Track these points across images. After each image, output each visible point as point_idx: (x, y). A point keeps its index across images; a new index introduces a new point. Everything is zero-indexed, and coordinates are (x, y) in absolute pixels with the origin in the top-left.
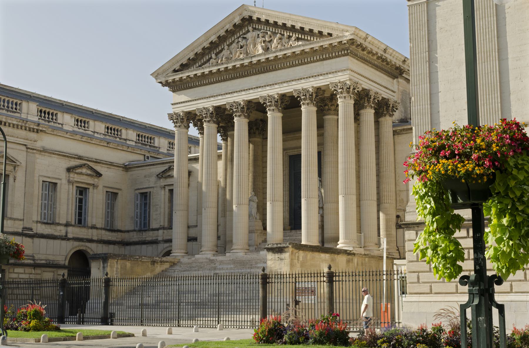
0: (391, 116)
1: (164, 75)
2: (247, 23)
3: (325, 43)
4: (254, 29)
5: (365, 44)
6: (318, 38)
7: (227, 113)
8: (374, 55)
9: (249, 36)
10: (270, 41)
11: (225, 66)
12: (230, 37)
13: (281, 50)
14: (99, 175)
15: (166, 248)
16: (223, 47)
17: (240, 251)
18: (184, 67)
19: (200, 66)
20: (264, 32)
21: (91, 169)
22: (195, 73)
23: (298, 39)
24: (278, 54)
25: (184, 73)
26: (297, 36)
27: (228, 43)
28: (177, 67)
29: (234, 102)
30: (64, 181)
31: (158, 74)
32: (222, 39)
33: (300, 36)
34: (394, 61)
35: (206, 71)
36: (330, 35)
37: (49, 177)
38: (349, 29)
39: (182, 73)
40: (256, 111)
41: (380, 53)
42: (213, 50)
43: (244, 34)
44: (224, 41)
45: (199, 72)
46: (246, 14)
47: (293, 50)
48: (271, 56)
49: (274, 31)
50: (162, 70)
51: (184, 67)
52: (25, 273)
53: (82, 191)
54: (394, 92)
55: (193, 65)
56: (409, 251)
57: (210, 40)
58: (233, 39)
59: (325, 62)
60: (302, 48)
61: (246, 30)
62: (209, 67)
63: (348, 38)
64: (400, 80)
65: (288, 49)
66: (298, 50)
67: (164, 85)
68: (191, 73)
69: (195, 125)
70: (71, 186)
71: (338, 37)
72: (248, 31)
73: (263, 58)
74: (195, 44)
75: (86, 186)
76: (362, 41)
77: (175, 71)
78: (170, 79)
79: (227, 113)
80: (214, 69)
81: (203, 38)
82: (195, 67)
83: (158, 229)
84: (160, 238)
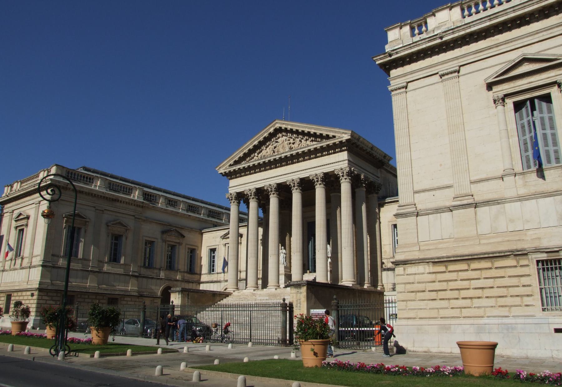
0: (377, 193)
1: (224, 168)
3: (330, 142)
5: (359, 143)
7: (265, 193)
8: (364, 151)
9: (279, 140)
10: (293, 143)
11: (264, 160)
14: (183, 236)
21: (178, 232)
22: (243, 166)
23: (312, 141)
24: (299, 151)
28: (232, 162)
30: (160, 240)
34: (378, 156)
35: (251, 164)
36: (334, 137)
37: (150, 237)
40: (284, 190)
41: (369, 150)
43: (277, 139)
47: (309, 148)
48: (294, 153)
52: (131, 301)
53: (173, 247)
54: (377, 177)
59: (331, 156)
60: (315, 146)
64: (383, 170)
65: (306, 147)
66: (312, 148)
67: (223, 175)
68: (241, 166)
69: (244, 202)
70: (164, 244)
71: (340, 138)
72: (279, 138)
73: (288, 154)
75: (175, 244)
76: (356, 141)
77: (230, 165)
78: (227, 171)
79: (265, 193)
80: (256, 163)
83: (221, 273)
84: (222, 279)
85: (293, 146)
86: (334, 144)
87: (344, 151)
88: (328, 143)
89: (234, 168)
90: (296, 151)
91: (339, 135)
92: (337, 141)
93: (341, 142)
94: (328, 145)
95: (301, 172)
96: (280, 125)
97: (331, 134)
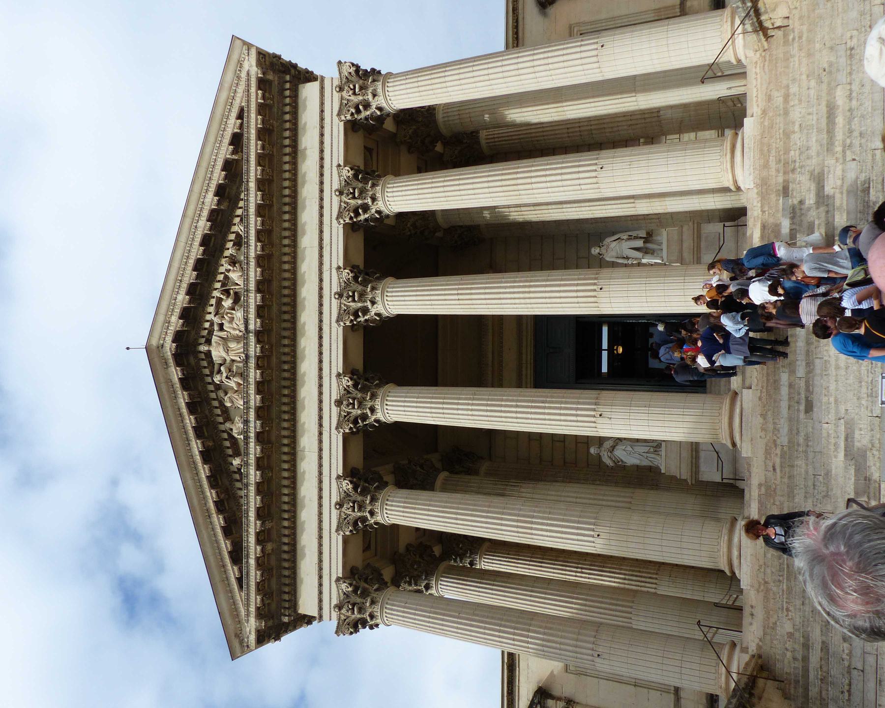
2: (192, 360)
4: (209, 342)
12: (211, 411)
16: (225, 436)
18: (237, 556)
25: (248, 547)
27: (221, 419)
28: (232, 572)
31: (237, 636)
35: (253, 476)
38: (235, 57)
39: (248, 556)
44: (216, 428)
50: (229, 621)
51: (237, 556)
57: (198, 458)
61: (205, 363)
63: (254, 63)
74: (195, 502)
78: (255, 599)
81: (188, 475)
87: (295, 96)
89: (252, 562)
93: (262, 83)
95: (326, 267)
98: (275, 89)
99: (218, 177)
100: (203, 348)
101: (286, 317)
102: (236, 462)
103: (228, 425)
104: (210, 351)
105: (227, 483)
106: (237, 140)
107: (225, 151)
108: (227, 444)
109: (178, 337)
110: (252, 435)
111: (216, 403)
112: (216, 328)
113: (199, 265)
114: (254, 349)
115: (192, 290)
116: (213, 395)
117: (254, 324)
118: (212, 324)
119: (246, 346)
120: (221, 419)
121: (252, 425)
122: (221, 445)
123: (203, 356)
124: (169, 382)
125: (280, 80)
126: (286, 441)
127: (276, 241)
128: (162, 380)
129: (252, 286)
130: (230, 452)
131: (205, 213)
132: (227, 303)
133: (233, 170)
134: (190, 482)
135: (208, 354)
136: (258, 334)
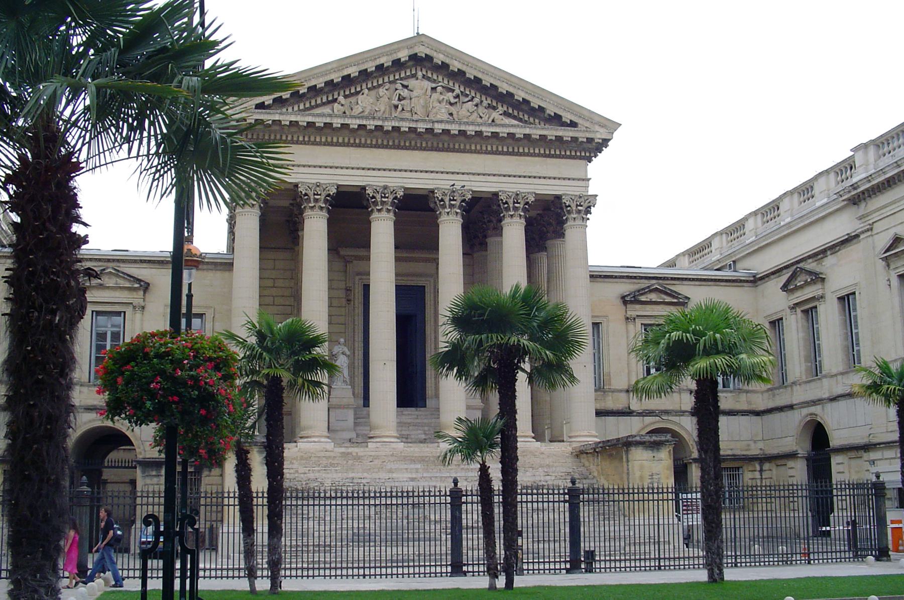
3: (567, 133)
6: (542, 123)
9: (412, 83)
12: (375, 77)
13: (490, 125)
15: (90, 421)
16: (358, 89)
17: (392, 440)
19: (306, 109)
20: (443, 87)
22: (310, 119)
23: (506, 114)
24: (484, 129)
25: (287, 114)
26: (505, 109)
27: (370, 86)
29: (385, 187)
32: (365, 75)
33: (510, 111)
36: (573, 124)
42: (340, 89)
43: (407, 78)
45: (320, 122)
46: (422, 51)
49: (462, 89)
55: (293, 105)
56: (792, 456)
57: (345, 73)
58: (381, 82)
62: (330, 116)
71: (587, 129)
74: (316, 71)
81: (335, 66)
82: (296, 108)
85: (453, 109)
86: (575, 139)
88: (560, 134)
90: (478, 129)
91: (587, 124)
92: (582, 136)
93: (590, 140)
94: (559, 139)
96: (428, 52)
97: (567, 117)
98: (585, 145)
99: (535, 103)
100: (420, 74)
101: (440, 146)
102: (341, 98)
103: (366, 91)
104: (417, 79)
105: (326, 90)
106: (556, 119)
107: (551, 110)
108: (353, 91)
109: (429, 58)
110: (364, 123)
111: (381, 82)
112: (434, 85)
113: (478, 80)
114: (421, 127)
115: (461, 73)
116: (386, 79)
117: (438, 128)
118: (434, 81)
119: (424, 121)
120: (370, 86)
121: (372, 122)
122: (352, 85)
123: (413, 72)
124: (399, 50)
125: (591, 148)
126: (357, 141)
127: (491, 141)
128: (400, 45)
129: (463, 128)
130: (347, 93)
131: (511, 90)
132: (450, 96)
133: (538, 113)
134: (330, 67)
135: (414, 76)
136: (432, 129)
